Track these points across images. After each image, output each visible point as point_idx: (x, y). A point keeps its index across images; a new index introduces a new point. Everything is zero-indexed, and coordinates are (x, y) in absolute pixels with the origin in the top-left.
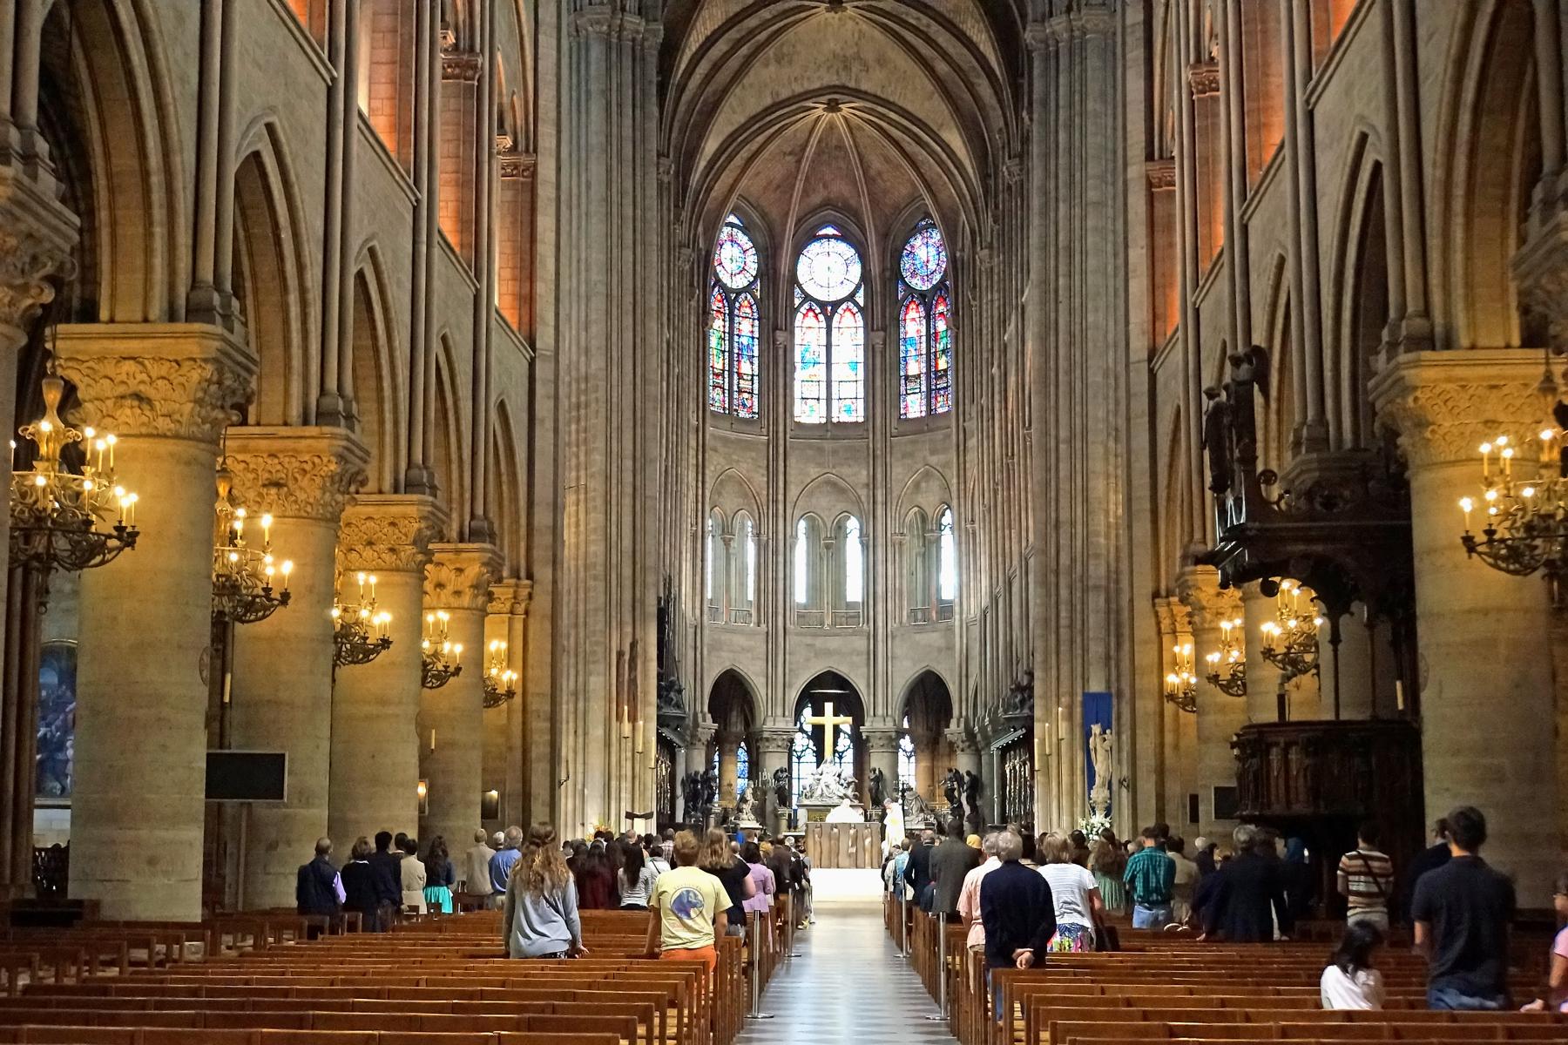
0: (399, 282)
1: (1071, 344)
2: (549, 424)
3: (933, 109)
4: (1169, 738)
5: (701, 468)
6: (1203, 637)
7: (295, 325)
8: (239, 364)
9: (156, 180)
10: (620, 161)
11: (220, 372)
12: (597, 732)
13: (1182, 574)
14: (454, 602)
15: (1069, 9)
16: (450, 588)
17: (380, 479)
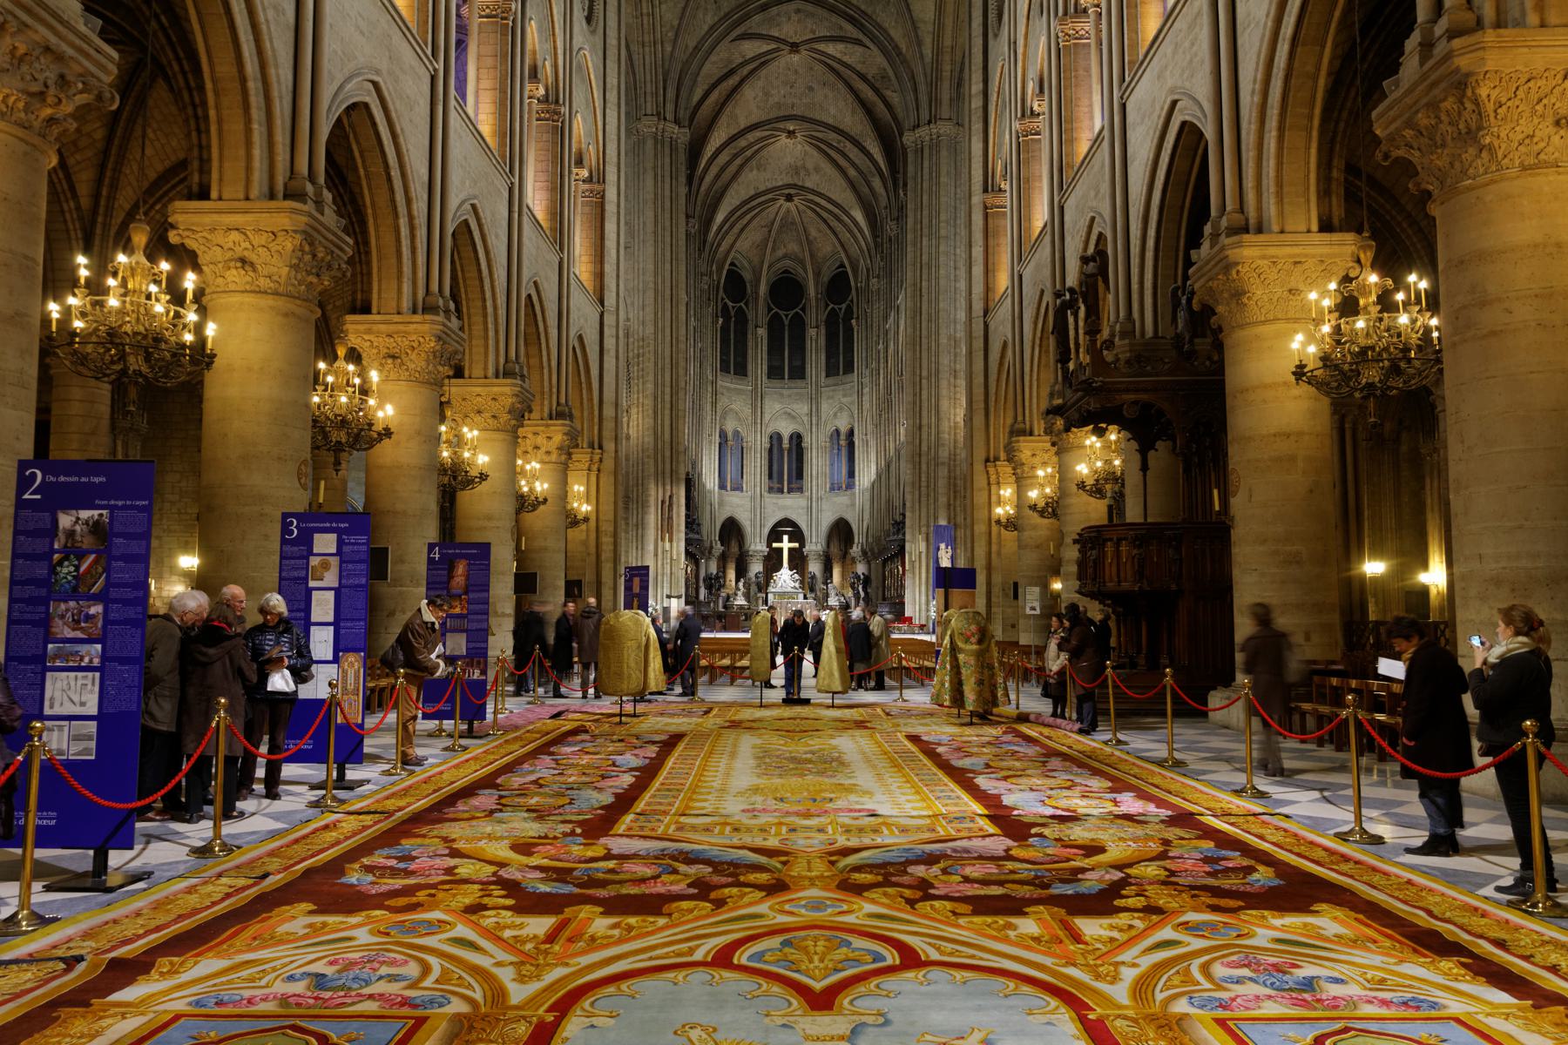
0: (497, 236)
1: (929, 321)
2: (613, 353)
3: (844, 196)
4: (994, 548)
5: (714, 404)
6: (1021, 482)
7: (405, 243)
8: (331, 242)
9: (253, 86)
10: (663, 209)
11: (311, 244)
12: (651, 547)
13: (1010, 443)
14: (546, 458)
15: (930, 122)
16: (543, 449)
17: (486, 368)
